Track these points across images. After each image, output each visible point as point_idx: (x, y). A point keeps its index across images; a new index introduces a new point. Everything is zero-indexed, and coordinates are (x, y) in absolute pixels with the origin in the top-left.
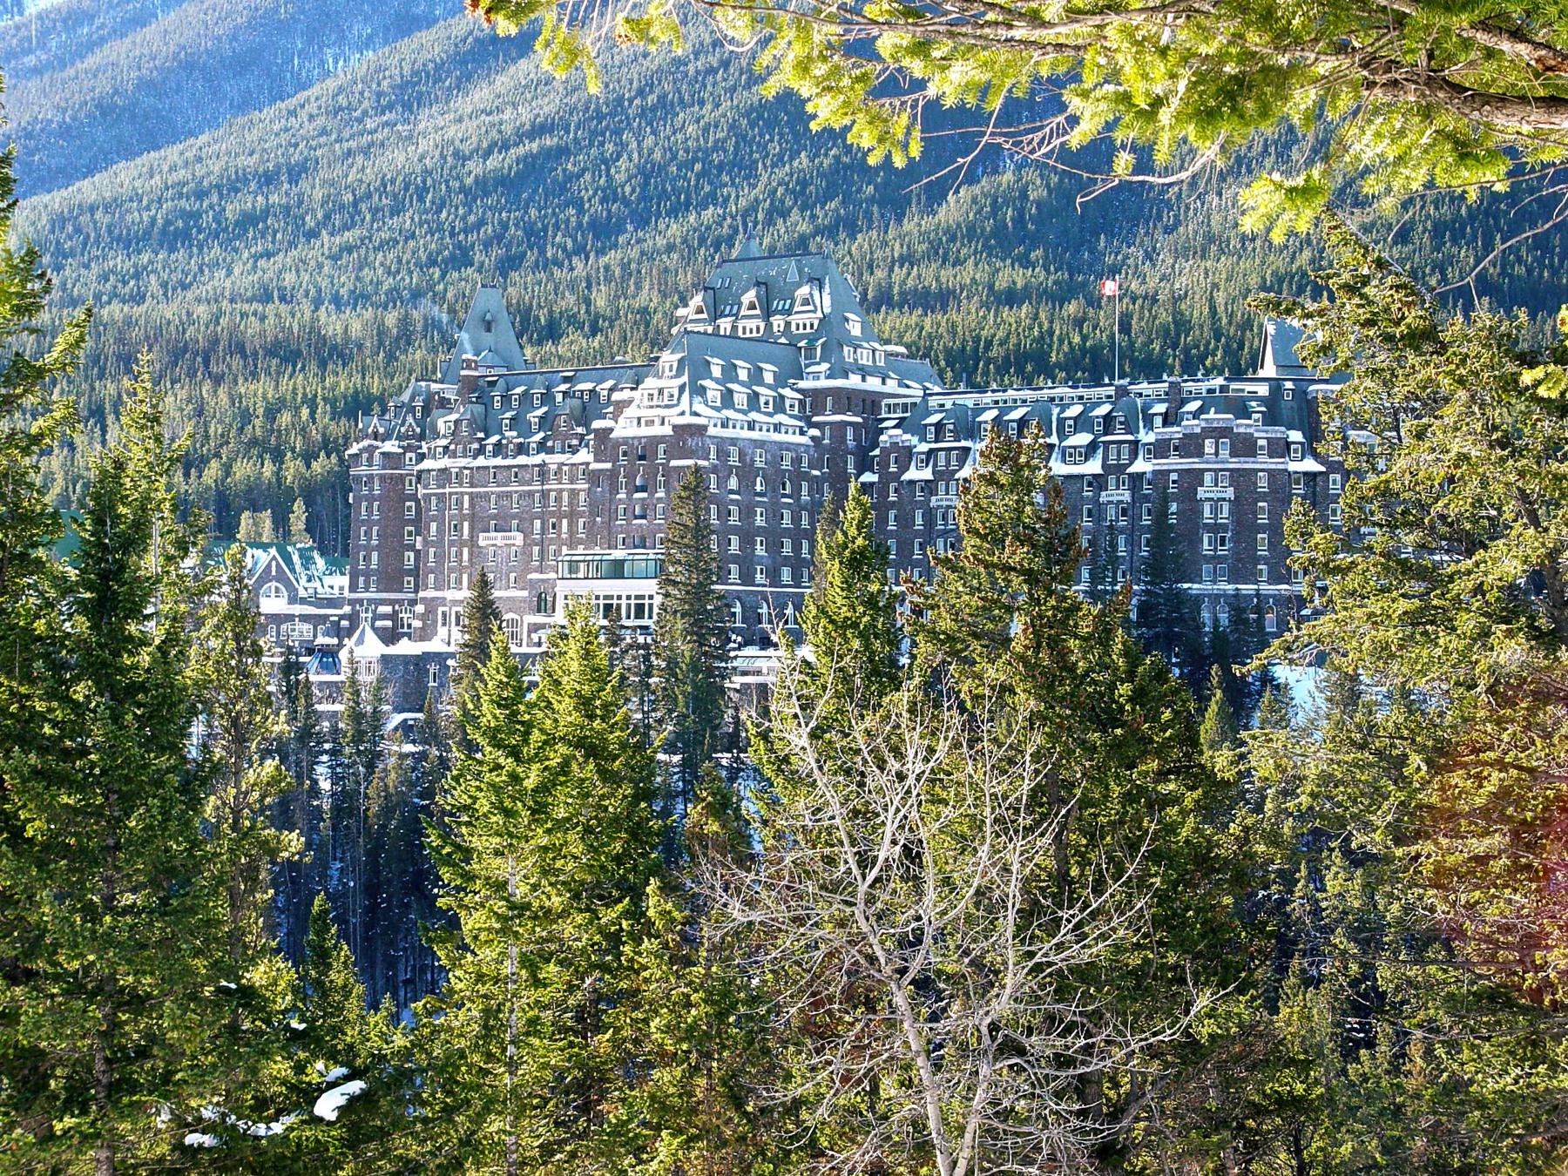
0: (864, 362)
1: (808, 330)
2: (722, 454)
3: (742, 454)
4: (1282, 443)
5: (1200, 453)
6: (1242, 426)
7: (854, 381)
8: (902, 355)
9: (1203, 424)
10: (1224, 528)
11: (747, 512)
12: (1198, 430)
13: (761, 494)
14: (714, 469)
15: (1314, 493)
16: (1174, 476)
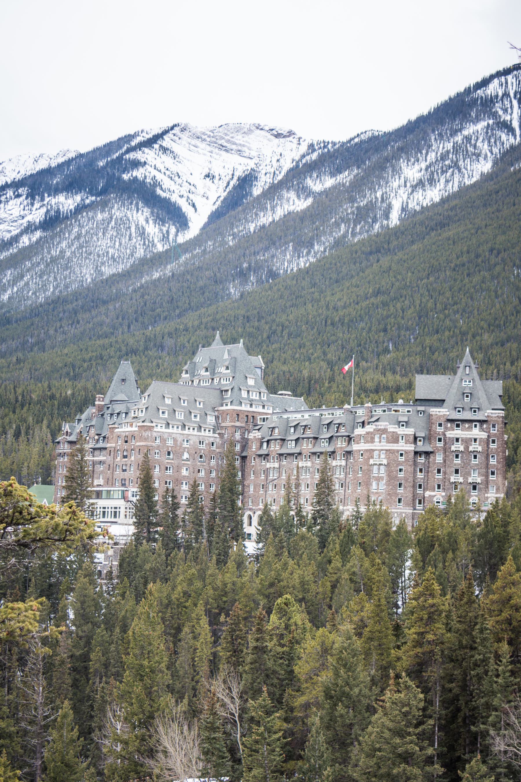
0: (254, 397)
1: (228, 382)
2: (163, 440)
3: (175, 440)
4: (412, 438)
5: (372, 441)
6: (392, 428)
7: (245, 408)
8: (289, 395)
9: (374, 427)
10: (382, 478)
11: (178, 469)
12: (372, 430)
13: (187, 460)
14: (158, 447)
15: (429, 462)
16: (362, 452)
